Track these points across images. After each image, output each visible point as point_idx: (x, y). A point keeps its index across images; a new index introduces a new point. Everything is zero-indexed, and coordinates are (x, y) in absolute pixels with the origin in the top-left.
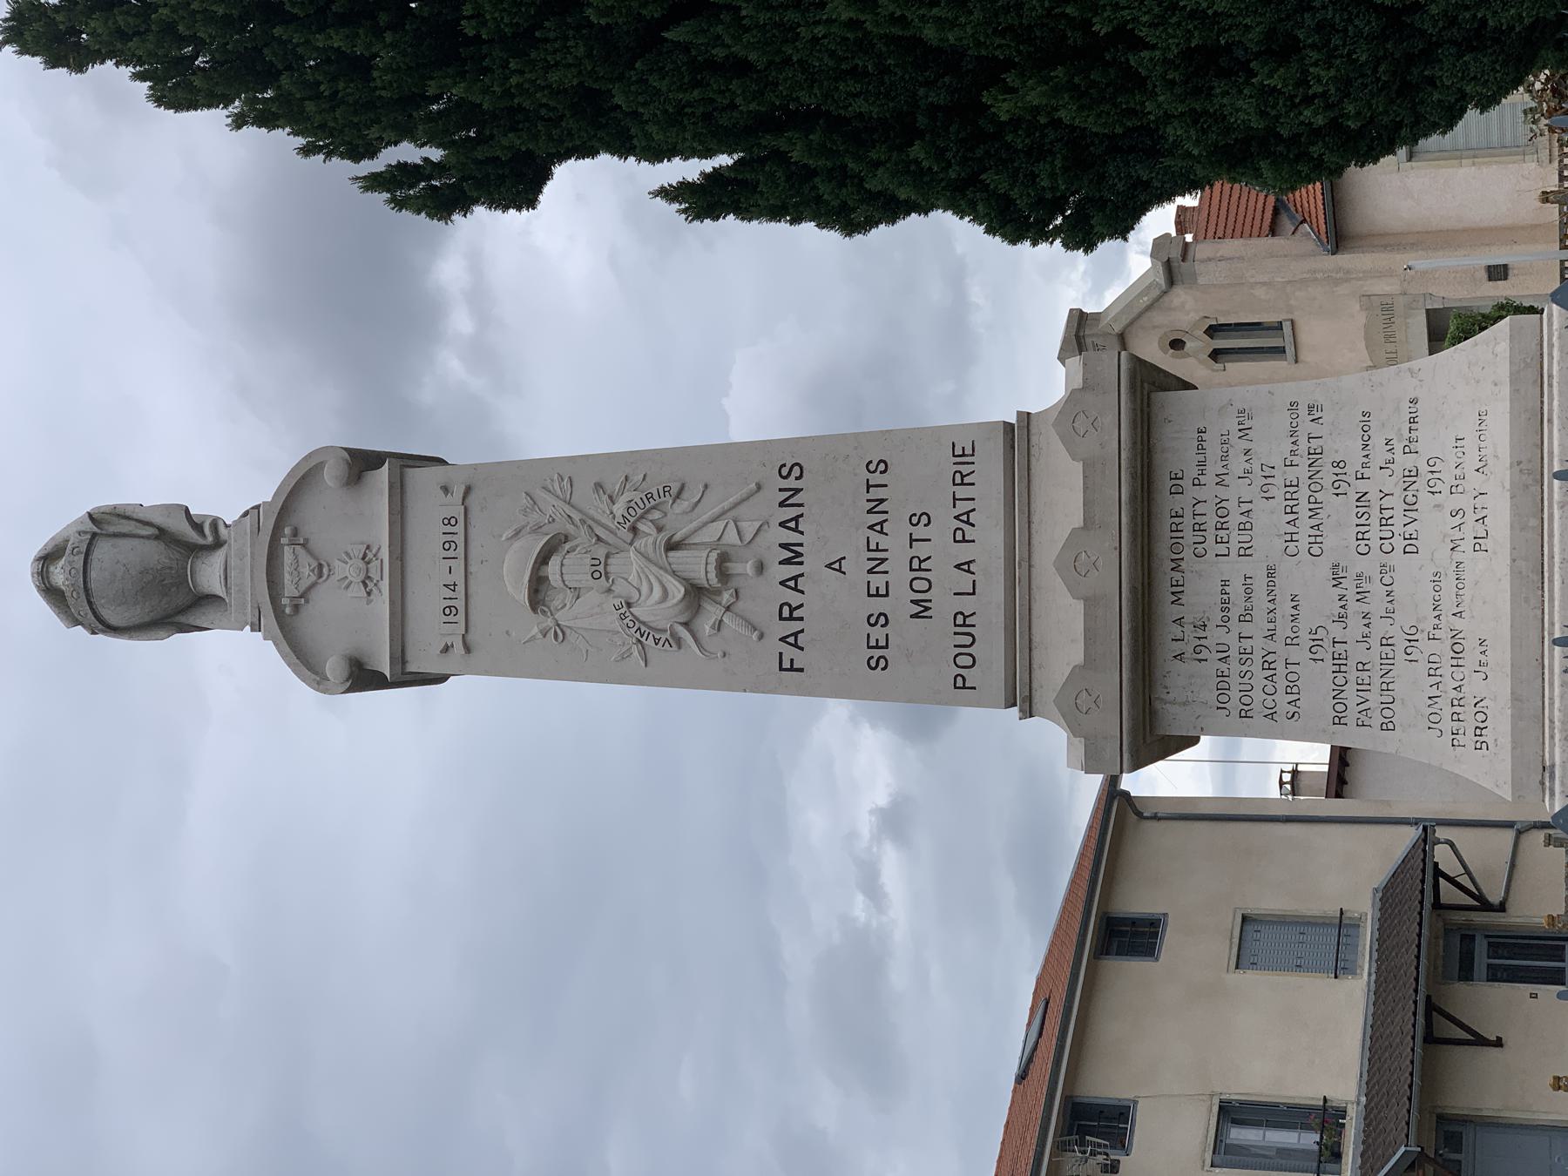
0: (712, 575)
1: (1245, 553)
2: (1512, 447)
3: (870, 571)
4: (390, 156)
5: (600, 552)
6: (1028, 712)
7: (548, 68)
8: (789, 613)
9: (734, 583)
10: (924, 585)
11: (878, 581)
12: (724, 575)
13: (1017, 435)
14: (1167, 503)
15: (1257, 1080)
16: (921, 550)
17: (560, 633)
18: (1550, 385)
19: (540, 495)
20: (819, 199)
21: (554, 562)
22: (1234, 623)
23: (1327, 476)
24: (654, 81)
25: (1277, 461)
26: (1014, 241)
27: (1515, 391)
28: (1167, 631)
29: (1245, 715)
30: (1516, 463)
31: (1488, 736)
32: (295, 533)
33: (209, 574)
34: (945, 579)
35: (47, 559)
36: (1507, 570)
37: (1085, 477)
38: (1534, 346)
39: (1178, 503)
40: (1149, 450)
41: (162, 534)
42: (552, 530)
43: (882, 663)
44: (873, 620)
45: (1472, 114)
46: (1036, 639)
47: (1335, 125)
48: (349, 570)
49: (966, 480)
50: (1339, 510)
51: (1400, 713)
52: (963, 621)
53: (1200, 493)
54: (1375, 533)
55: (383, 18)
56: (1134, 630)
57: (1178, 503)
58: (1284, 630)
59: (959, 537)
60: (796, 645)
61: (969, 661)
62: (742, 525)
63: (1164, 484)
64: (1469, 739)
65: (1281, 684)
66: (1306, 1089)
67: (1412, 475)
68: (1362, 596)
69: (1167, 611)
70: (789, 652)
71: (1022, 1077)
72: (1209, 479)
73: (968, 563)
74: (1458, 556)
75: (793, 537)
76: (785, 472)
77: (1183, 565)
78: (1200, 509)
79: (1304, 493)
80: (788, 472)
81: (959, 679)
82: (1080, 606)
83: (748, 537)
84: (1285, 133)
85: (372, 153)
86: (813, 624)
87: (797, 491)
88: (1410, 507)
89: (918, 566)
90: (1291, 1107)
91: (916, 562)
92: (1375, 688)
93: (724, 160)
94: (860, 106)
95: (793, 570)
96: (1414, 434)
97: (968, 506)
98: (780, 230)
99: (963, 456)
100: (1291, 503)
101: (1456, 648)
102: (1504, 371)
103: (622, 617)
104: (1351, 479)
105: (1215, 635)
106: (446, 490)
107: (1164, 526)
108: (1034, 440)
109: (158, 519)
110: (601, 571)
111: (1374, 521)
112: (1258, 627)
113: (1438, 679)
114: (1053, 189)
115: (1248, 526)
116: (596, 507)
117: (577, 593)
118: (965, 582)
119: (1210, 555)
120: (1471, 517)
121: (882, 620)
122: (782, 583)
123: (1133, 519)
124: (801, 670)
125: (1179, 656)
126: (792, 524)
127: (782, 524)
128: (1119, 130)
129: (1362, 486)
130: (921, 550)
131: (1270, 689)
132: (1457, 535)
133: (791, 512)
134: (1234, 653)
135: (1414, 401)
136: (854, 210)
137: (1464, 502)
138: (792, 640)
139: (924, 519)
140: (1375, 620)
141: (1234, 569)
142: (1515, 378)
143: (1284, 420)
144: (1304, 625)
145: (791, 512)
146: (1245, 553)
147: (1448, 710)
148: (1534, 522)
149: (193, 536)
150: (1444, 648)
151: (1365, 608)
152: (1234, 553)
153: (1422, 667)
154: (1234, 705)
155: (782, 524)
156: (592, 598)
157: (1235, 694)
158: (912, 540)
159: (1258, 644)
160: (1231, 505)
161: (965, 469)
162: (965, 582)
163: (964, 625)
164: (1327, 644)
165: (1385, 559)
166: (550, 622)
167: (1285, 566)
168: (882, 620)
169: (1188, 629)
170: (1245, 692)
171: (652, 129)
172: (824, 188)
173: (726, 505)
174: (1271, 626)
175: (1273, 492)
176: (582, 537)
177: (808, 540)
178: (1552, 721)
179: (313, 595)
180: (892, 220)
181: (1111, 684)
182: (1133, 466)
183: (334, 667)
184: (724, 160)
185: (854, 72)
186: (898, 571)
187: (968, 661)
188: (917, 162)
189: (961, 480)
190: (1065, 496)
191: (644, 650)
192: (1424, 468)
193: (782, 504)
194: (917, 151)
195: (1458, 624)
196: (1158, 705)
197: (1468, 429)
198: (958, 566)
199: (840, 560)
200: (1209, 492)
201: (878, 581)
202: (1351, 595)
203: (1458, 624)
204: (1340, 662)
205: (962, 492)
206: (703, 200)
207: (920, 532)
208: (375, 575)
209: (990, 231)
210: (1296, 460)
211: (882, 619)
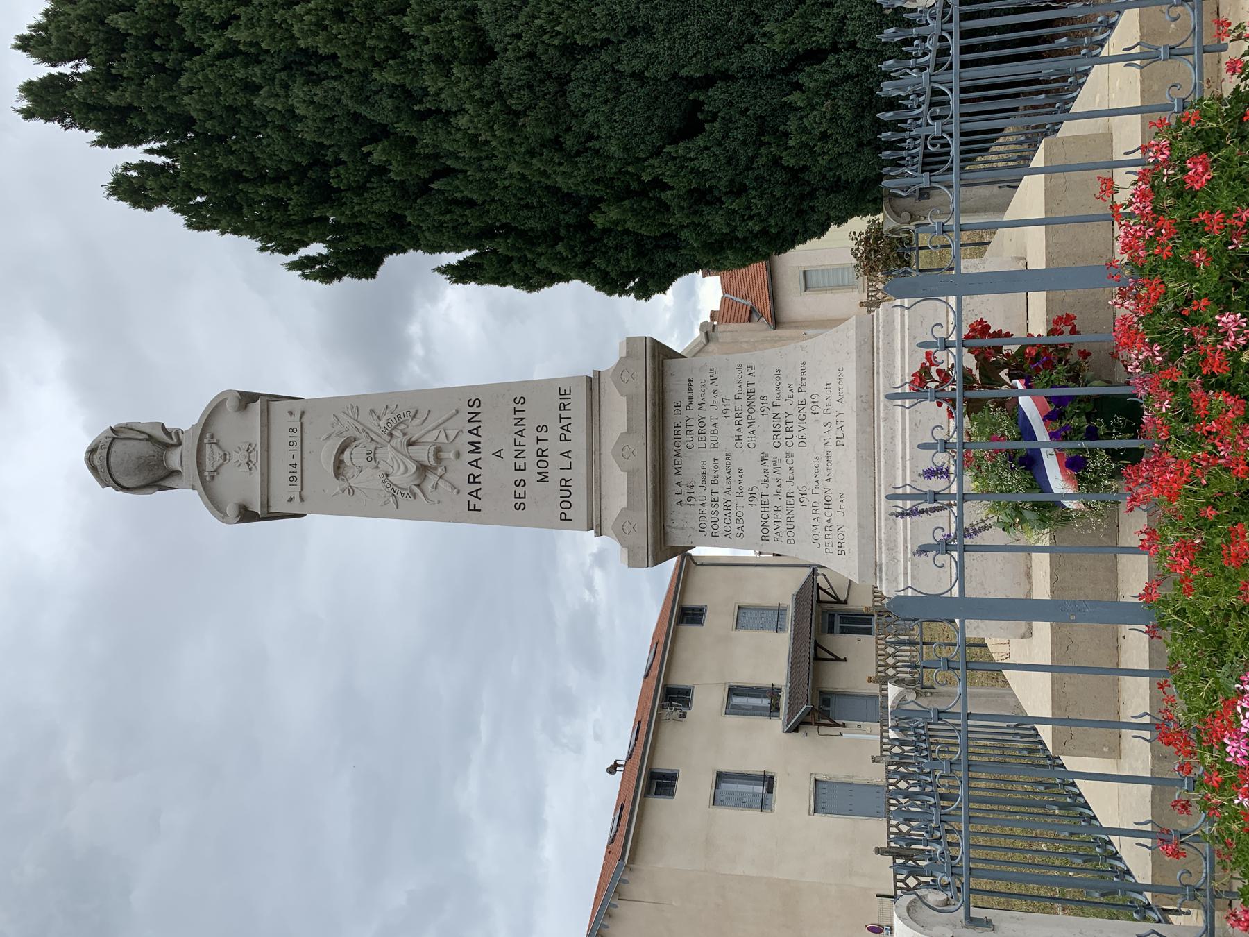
0: (432, 459)
4: (303, 252)
5: (372, 447)
7: (373, 202)
8: (473, 479)
9: (443, 463)
11: (520, 462)
12: (438, 459)
13: (593, 383)
14: (672, 419)
15: (744, 677)
16: (543, 445)
17: (351, 491)
19: (341, 416)
20: (514, 274)
21: (347, 452)
22: (708, 485)
23: (757, 404)
24: (427, 209)
26: (610, 294)
27: (859, 357)
28: (673, 489)
31: (845, 547)
32: (212, 437)
33: (173, 460)
34: (556, 461)
35: (92, 451)
38: (870, 333)
41: (150, 438)
42: (347, 435)
45: (833, 228)
47: (764, 232)
48: (240, 457)
50: (764, 424)
52: (565, 484)
54: (783, 435)
55: (292, 179)
56: (654, 488)
63: (671, 409)
64: (835, 549)
65: (734, 518)
66: (765, 680)
67: (802, 404)
69: (673, 478)
70: (473, 501)
71: (646, 676)
72: (695, 406)
74: (828, 448)
75: (476, 439)
78: (690, 423)
79: (745, 414)
80: (474, 403)
82: (625, 475)
84: (740, 236)
85: (295, 251)
88: (802, 421)
89: (541, 453)
92: (784, 520)
93: (467, 253)
94: (531, 224)
95: (476, 456)
97: (568, 421)
98: (494, 289)
99: (564, 395)
102: (852, 346)
103: (384, 482)
104: (770, 406)
105: (698, 491)
106: (291, 413)
108: (602, 385)
109: (148, 431)
110: (372, 457)
114: (628, 267)
116: (370, 422)
117: (361, 469)
118: (565, 462)
119: (696, 447)
120: (834, 427)
125: (679, 503)
126: (475, 432)
128: (658, 234)
129: (776, 410)
130: (543, 445)
133: (475, 425)
134: (708, 501)
137: (831, 418)
138: (475, 494)
141: (708, 455)
143: (734, 375)
145: (475, 425)
148: (869, 429)
149: (166, 439)
150: (820, 498)
153: (809, 509)
154: (709, 529)
156: (368, 471)
157: (709, 523)
159: (721, 497)
160: (707, 420)
161: (566, 402)
164: (758, 496)
166: (346, 485)
167: (735, 454)
169: (684, 488)
171: (427, 234)
172: (516, 267)
175: (729, 413)
176: (363, 439)
179: (222, 470)
181: (642, 518)
183: (231, 510)
184: (467, 253)
185: (527, 206)
186: (531, 458)
188: (560, 253)
189: (564, 407)
190: (621, 416)
191: (396, 500)
192: (809, 400)
194: (560, 247)
196: (668, 529)
201: (520, 462)
202: (771, 470)
204: (764, 506)
205: (564, 414)
207: (542, 435)
208: (253, 459)
209: (598, 289)
211: (523, 482)
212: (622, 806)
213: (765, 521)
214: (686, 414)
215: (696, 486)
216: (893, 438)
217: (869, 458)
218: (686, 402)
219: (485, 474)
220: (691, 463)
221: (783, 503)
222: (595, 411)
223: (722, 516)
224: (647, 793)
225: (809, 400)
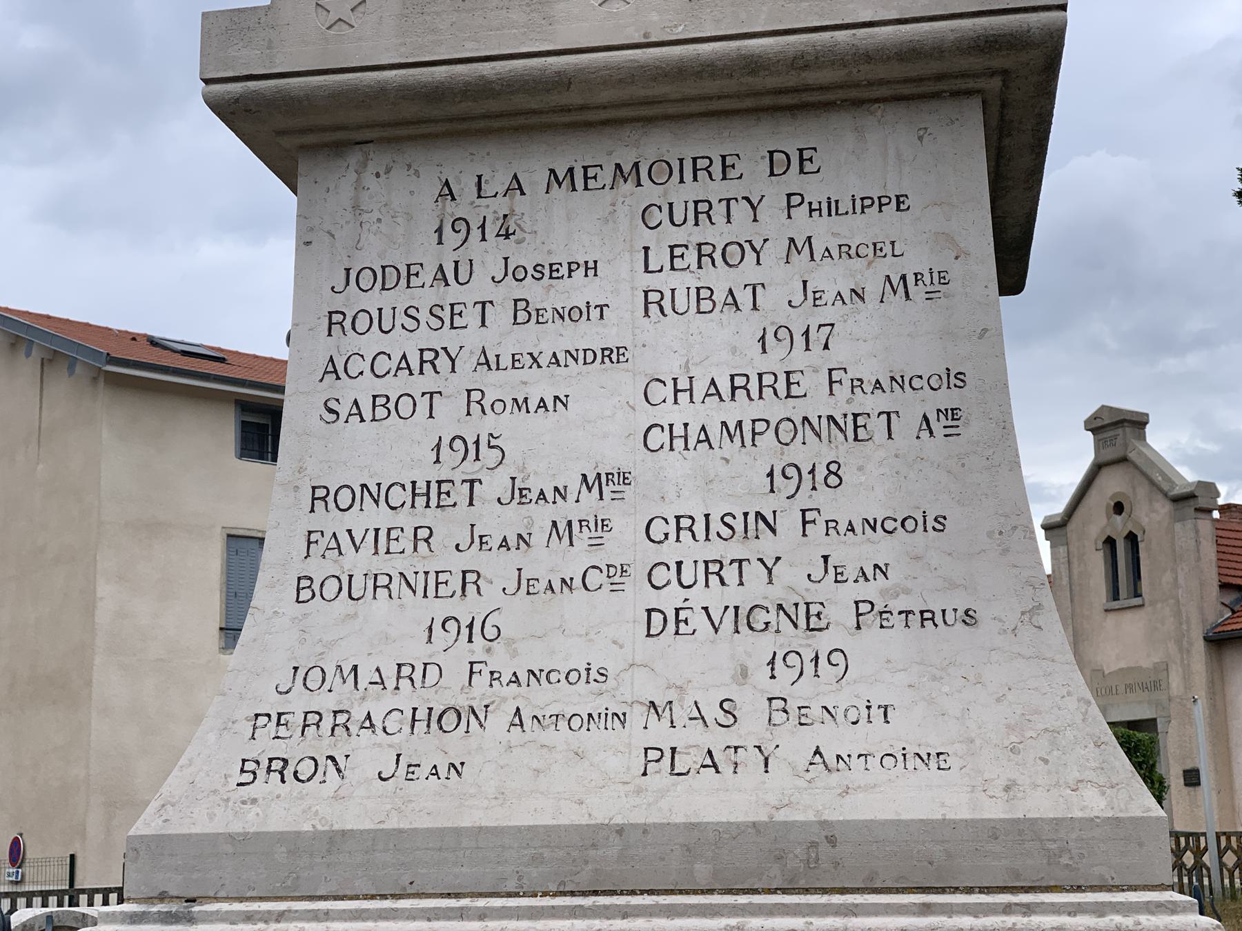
1: (652, 303)
2: (869, 825)
14: (750, 146)
18: (1008, 909)
25: (840, 353)
27: (993, 830)
29: (334, 321)
30: (830, 834)
36: (600, 818)
38: (1099, 872)
39: (751, 166)
40: (858, 103)
50: (738, 479)
53: (773, 210)
54: (691, 551)
56: (483, 89)
57: (751, 166)
58: (496, 385)
64: (266, 746)
67: (810, 619)
68: (564, 531)
72: (802, 223)
74: (637, 716)
77: (630, 185)
79: (773, 409)
88: (744, 618)
96: (898, 620)
100: (754, 386)
101: (450, 718)
102: (1040, 804)
104: (803, 500)
105: (488, 256)
107: (705, 143)
111: (715, 550)
112: (503, 336)
113: (390, 684)
119: (648, 238)
120: (717, 740)
125: (448, 193)
129: (789, 523)
131: (382, 365)
134: (454, 293)
135: (969, 617)
137: (751, 728)
140: (514, 558)
141: (620, 284)
144: (507, 425)
146: (652, 303)
147: (325, 702)
148: (702, 873)
150: (452, 692)
151: (538, 539)
153: (416, 652)
154: (354, 300)
157: (373, 301)
159: (471, 338)
160: (749, 271)
164: (470, 468)
167: (622, 383)
169: (501, 205)
170: (377, 320)
174: (506, 361)
175: (777, 351)
192: (824, 643)
195: (499, 720)
196: (354, 158)
197: (907, 730)
202: (565, 511)
203: (499, 720)
204: (434, 493)
210: (842, 391)
212: (222, 360)
213: (375, 494)
214: (773, 193)
215: (507, 247)
218: (816, 191)
224: (244, 405)
225: (824, 643)
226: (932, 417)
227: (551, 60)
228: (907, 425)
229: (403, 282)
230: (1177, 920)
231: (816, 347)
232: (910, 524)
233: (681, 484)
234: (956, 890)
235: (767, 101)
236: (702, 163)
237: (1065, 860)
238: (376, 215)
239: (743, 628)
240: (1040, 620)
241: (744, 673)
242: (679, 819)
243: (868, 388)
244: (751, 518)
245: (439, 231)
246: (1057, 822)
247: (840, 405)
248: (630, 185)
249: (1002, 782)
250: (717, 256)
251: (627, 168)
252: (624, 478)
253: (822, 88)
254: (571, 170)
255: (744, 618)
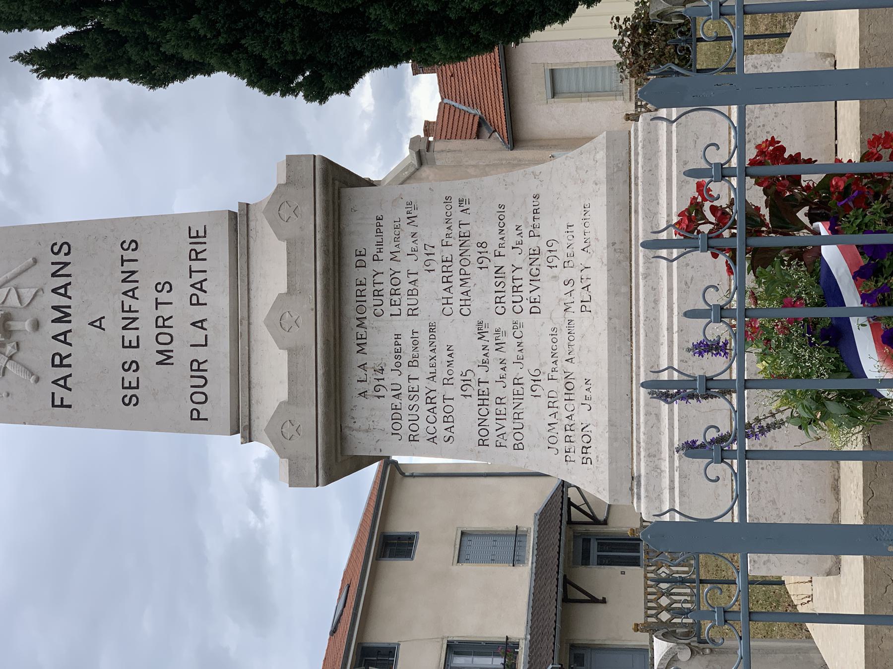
3: (124, 328)
6: (248, 438)
8: (60, 361)
9: (15, 338)
10: (167, 339)
11: (130, 335)
13: (238, 221)
14: (353, 274)
15: (468, 629)
16: (165, 311)
18: (636, 185)
20: (129, 61)
22: (404, 368)
23: (473, 254)
27: (610, 189)
29: (413, 439)
34: (183, 333)
36: (605, 326)
37: (288, 253)
40: (340, 233)
43: (134, 400)
44: (126, 367)
45: (581, 9)
46: (254, 380)
49: (200, 256)
50: (482, 281)
51: (528, 436)
52: (197, 367)
53: (378, 266)
54: (508, 298)
56: (327, 374)
58: (442, 373)
59: (194, 301)
60: (65, 387)
61: (201, 398)
62: (22, 291)
63: (351, 259)
64: (577, 456)
65: (440, 415)
66: (496, 632)
67: (535, 253)
70: (60, 392)
71: (334, 632)
72: (385, 255)
73: (202, 321)
74: (569, 316)
75: (64, 301)
76: (56, 249)
77: (366, 321)
78: (378, 279)
79: (456, 267)
80: (60, 250)
81: (195, 412)
82: (284, 354)
83: (27, 301)
84: (453, 16)
86: (78, 372)
87: (66, 264)
88: (534, 278)
89: (162, 323)
90: (487, 643)
91: (160, 320)
92: (509, 417)
95: (63, 327)
96: (537, 222)
97: (201, 276)
99: (197, 237)
100: (447, 274)
101: (569, 386)
102: (602, 173)
105: (390, 377)
107: (351, 291)
108: (252, 224)
111: (509, 289)
113: (555, 410)
114: (294, 53)
115: (415, 292)
118: (198, 336)
120: (578, 286)
121: (134, 366)
122: (55, 337)
123: (326, 287)
124: (70, 406)
125: (363, 394)
126: (62, 291)
127: (54, 291)
128: (337, 10)
129: (499, 261)
130: (165, 311)
132: (569, 299)
133: (62, 281)
134: (404, 391)
135: (536, 197)
136: (154, 68)
137: (574, 274)
138: (63, 383)
139: (167, 287)
141: (404, 326)
142: (610, 180)
143: (441, 210)
144: (457, 369)
145: (62, 281)
147: (562, 434)
148: (625, 289)
151: (502, 356)
152: (404, 313)
153: (544, 401)
154: (405, 431)
155: (54, 291)
157: (405, 423)
158: (157, 304)
159: (423, 384)
160: (402, 276)
161: (199, 248)
162: (198, 336)
163: (198, 370)
164: (474, 383)
165: (516, 317)
167: (443, 324)
168: (134, 366)
169: (370, 372)
172: (132, 51)
173: (9, 275)
174: (433, 370)
177: (75, 304)
178: (638, 442)
180: (183, 78)
181: (309, 416)
182: (325, 245)
186: (146, 329)
187: (201, 398)
188: (194, 29)
189: (196, 256)
190: (277, 270)
192: (544, 248)
193: (54, 275)
194: (194, 22)
195: (570, 367)
196: (347, 432)
197: (576, 218)
198: (193, 324)
199: (100, 319)
200: (385, 266)
201: (130, 335)
202: (492, 346)
203: (570, 367)
204: (483, 397)
205: (196, 265)
206: (53, 63)
207: (164, 297)
209: (251, 84)
210: (451, 241)
213: (483, 419)
214: (373, 266)
215: (387, 369)
216: (656, 302)
217: (623, 328)
218: (373, 250)
219: (77, 352)
220: (383, 336)
221: (508, 392)
222: (242, 263)
223: (423, 412)
225: (544, 248)
226: (462, 208)
227: (319, 346)
228: (464, 218)
229: (398, 411)
230: (640, 129)
231: (433, 251)
232: (501, 217)
233: (483, 301)
234: (630, 202)
235: (337, 267)
236: (359, 294)
237: (620, 165)
238: (371, 423)
239: (538, 278)
240: (538, 172)
241: (554, 277)
242: (606, 298)
243: (450, 232)
244: (497, 275)
245: (379, 397)
246: (608, 168)
247: (456, 242)
248: (366, 321)
249: (594, 186)
250: (396, 288)
251: (359, 323)
252: (480, 323)
253: (334, 247)
254: (358, 345)
255: (534, 278)
